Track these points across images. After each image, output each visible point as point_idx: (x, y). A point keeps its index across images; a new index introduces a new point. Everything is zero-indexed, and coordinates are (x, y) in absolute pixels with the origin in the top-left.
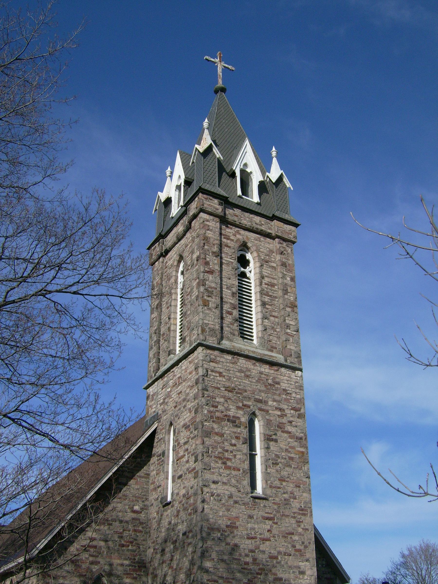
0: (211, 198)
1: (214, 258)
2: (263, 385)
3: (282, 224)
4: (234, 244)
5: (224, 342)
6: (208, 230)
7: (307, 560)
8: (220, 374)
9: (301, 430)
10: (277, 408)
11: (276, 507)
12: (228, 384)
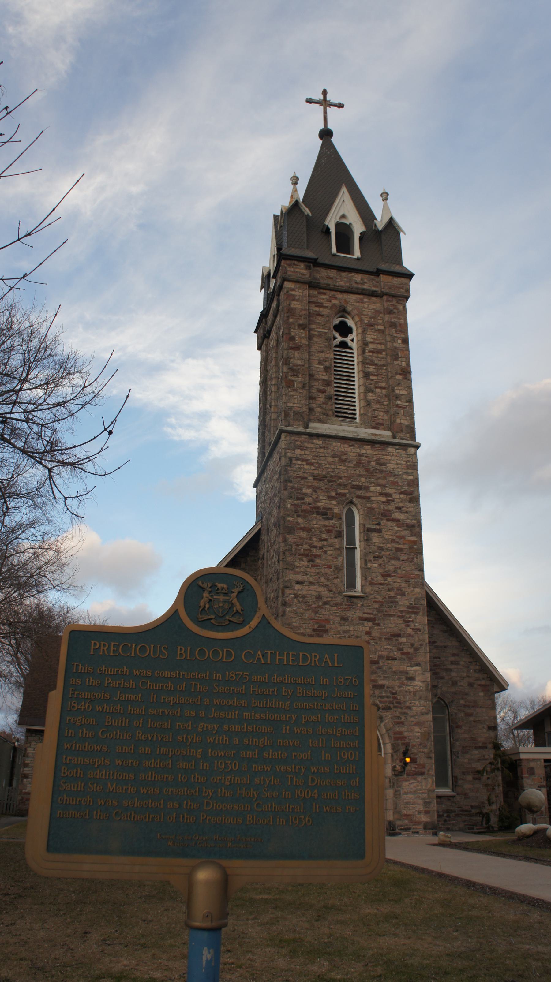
0: (296, 262)
1: (302, 331)
2: (363, 469)
3: (391, 277)
4: (329, 311)
5: (312, 425)
6: (293, 300)
7: (417, 665)
8: (308, 463)
9: (413, 516)
11: (377, 606)
12: (317, 472)
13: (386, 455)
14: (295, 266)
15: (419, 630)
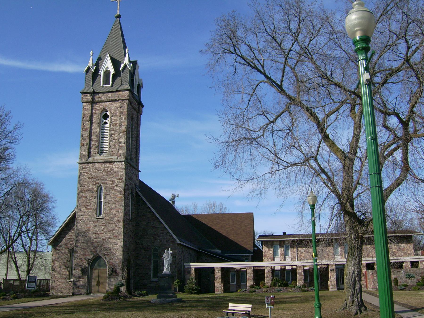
0: (87, 95)
8: (87, 173)
10: (111, 181)
12: (89, 176)
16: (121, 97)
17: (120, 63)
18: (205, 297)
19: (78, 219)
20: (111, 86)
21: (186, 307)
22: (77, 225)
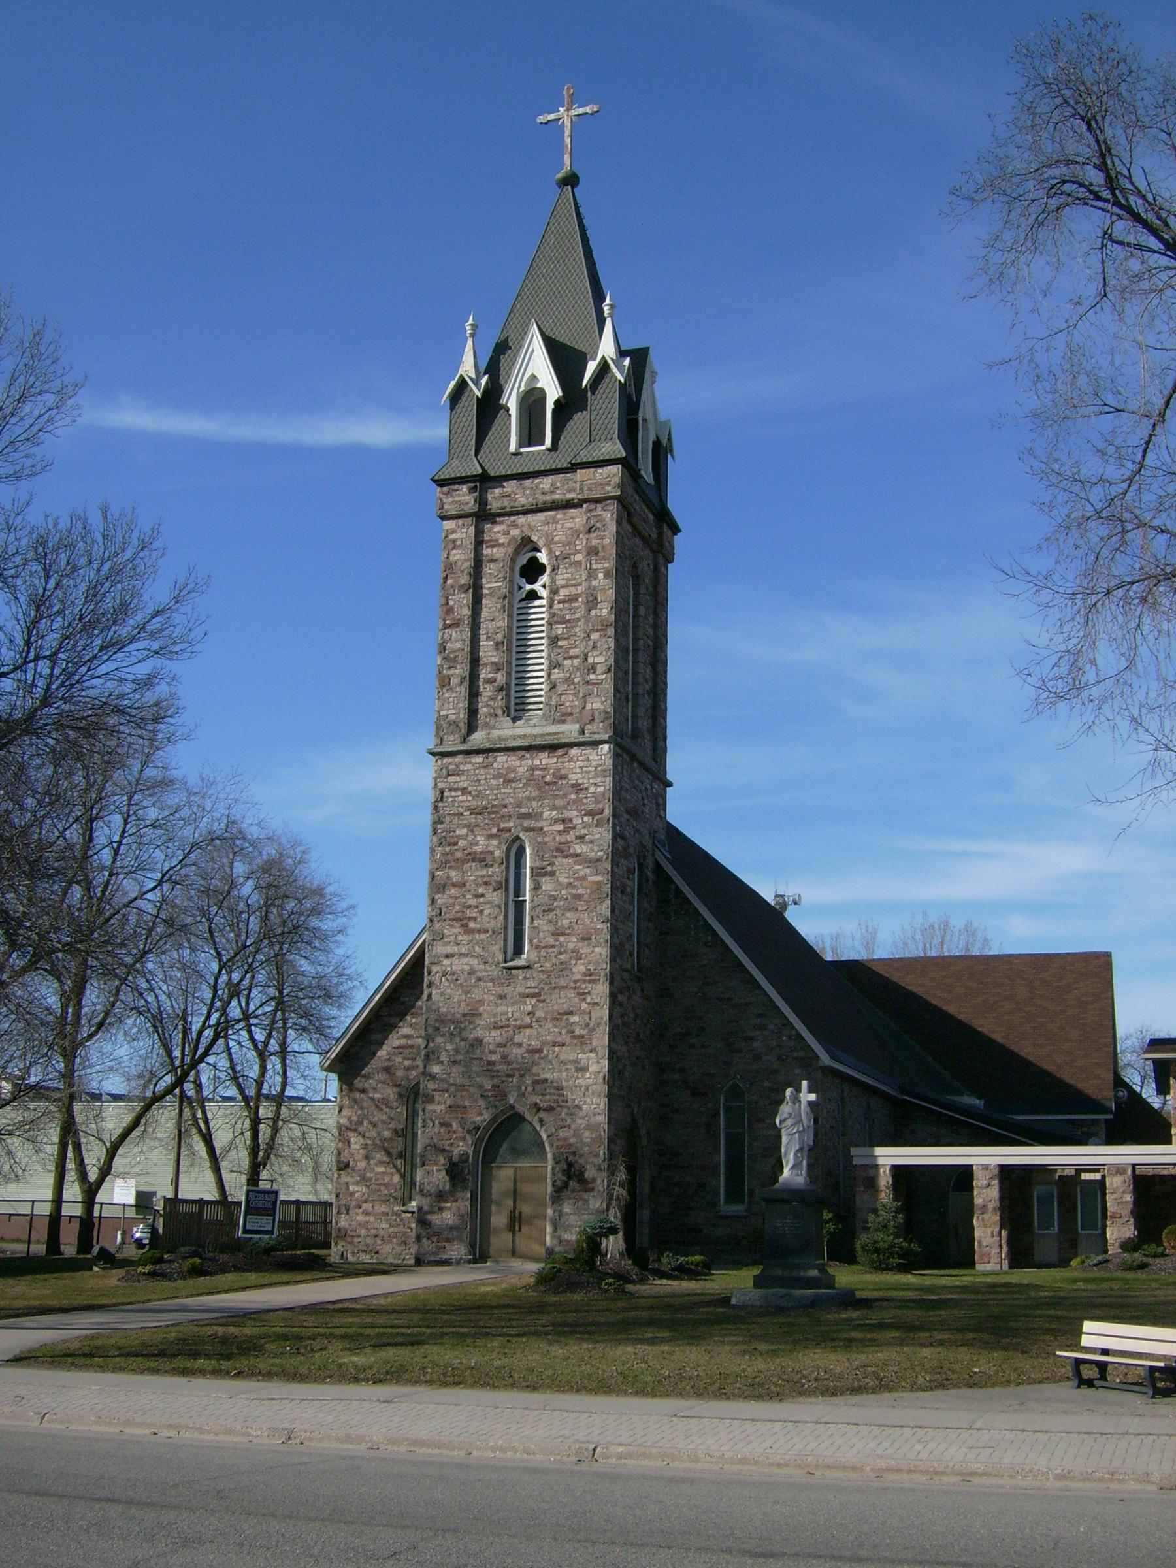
0: (456, 487)
1: (463, 595)
3: (592, 470)
8: (464, 791)
10: (556, 821)
11: (543, 977)
12: (474, 803)
13: (569, 762)
14: (454, 493)
15: (597, 1004)
16: (590, 489)
17: (581, 360)
18: (945, 1287)
19: (435, 969)
20: (549, 450)
21: (882, 1326)
22: (430, 996)
